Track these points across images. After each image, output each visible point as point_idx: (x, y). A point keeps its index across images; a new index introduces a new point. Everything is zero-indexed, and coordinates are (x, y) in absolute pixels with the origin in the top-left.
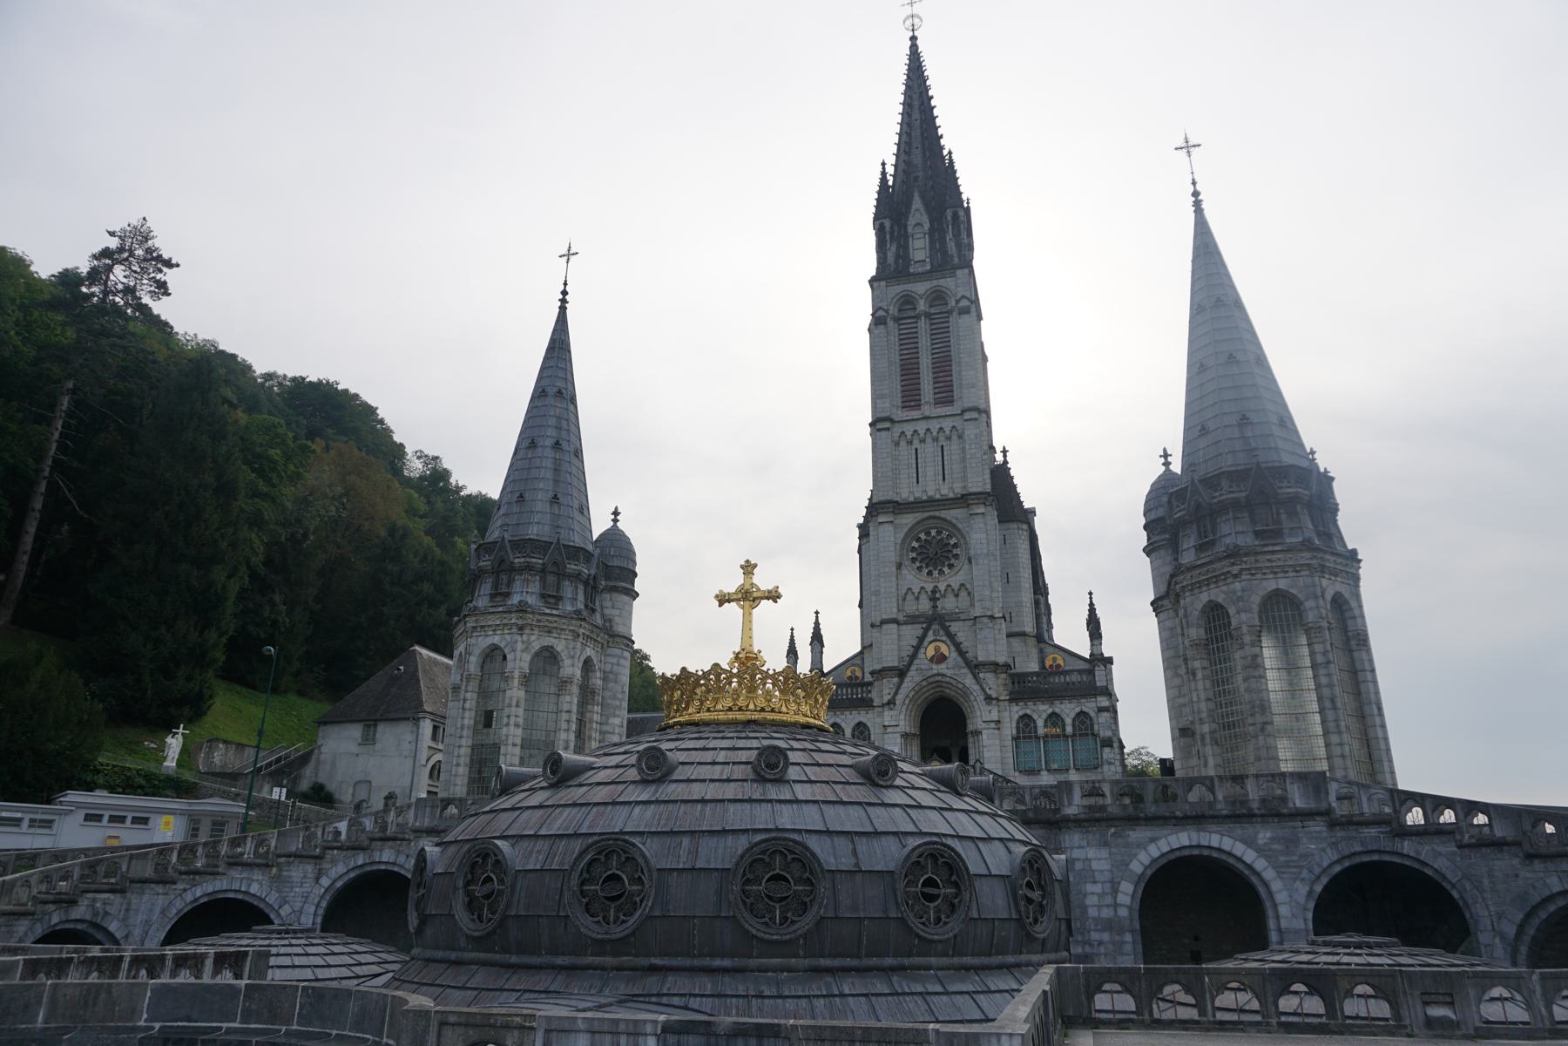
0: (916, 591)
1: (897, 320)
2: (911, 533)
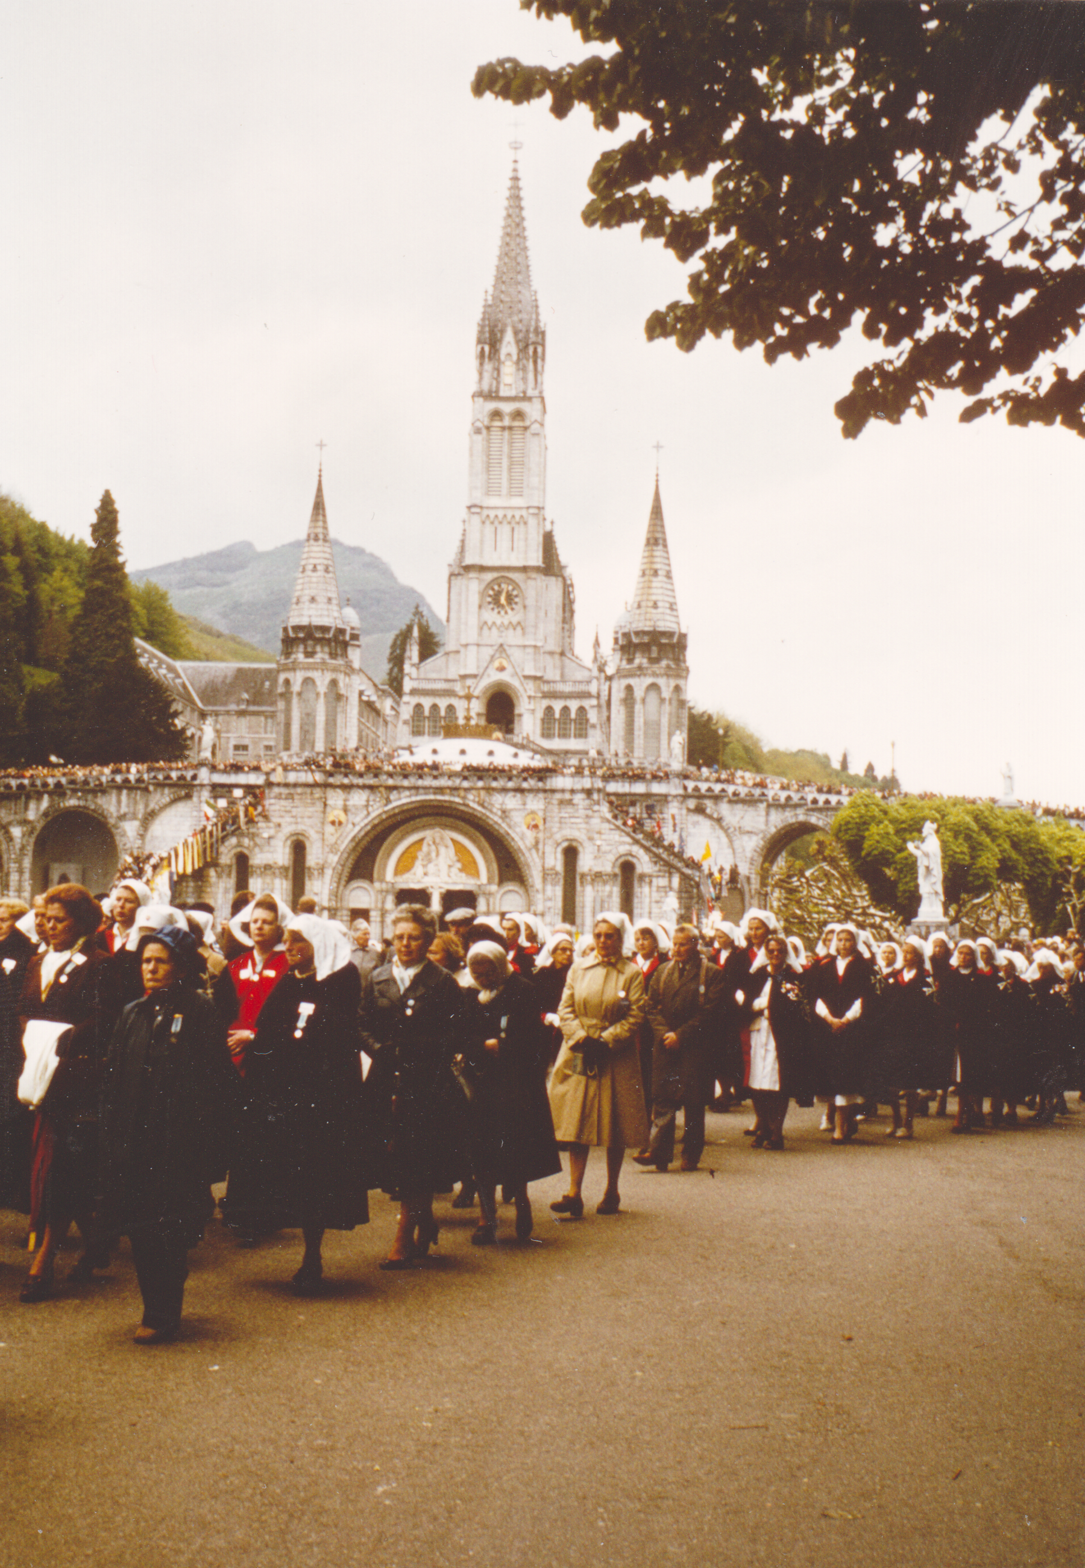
0: (490, 623)
1: (488, 428)
2: (490, 586)
